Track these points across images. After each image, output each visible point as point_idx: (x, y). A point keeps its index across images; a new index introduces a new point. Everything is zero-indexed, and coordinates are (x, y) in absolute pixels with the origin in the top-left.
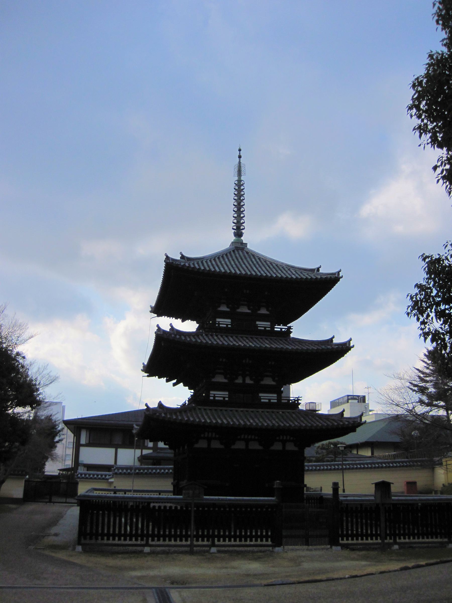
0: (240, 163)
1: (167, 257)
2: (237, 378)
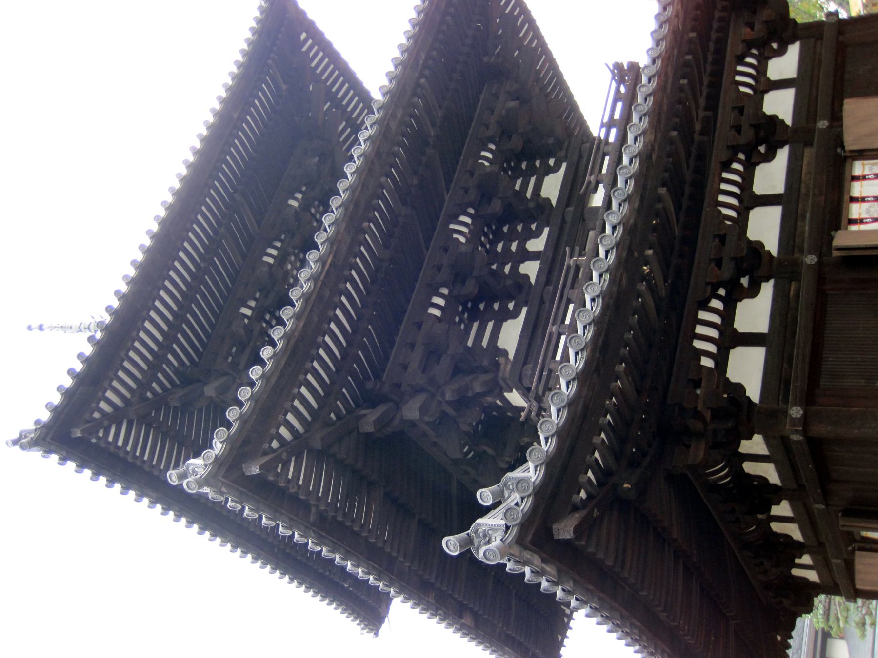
0: (51, 328)
1: (23, 442)
2: (527, 277)
